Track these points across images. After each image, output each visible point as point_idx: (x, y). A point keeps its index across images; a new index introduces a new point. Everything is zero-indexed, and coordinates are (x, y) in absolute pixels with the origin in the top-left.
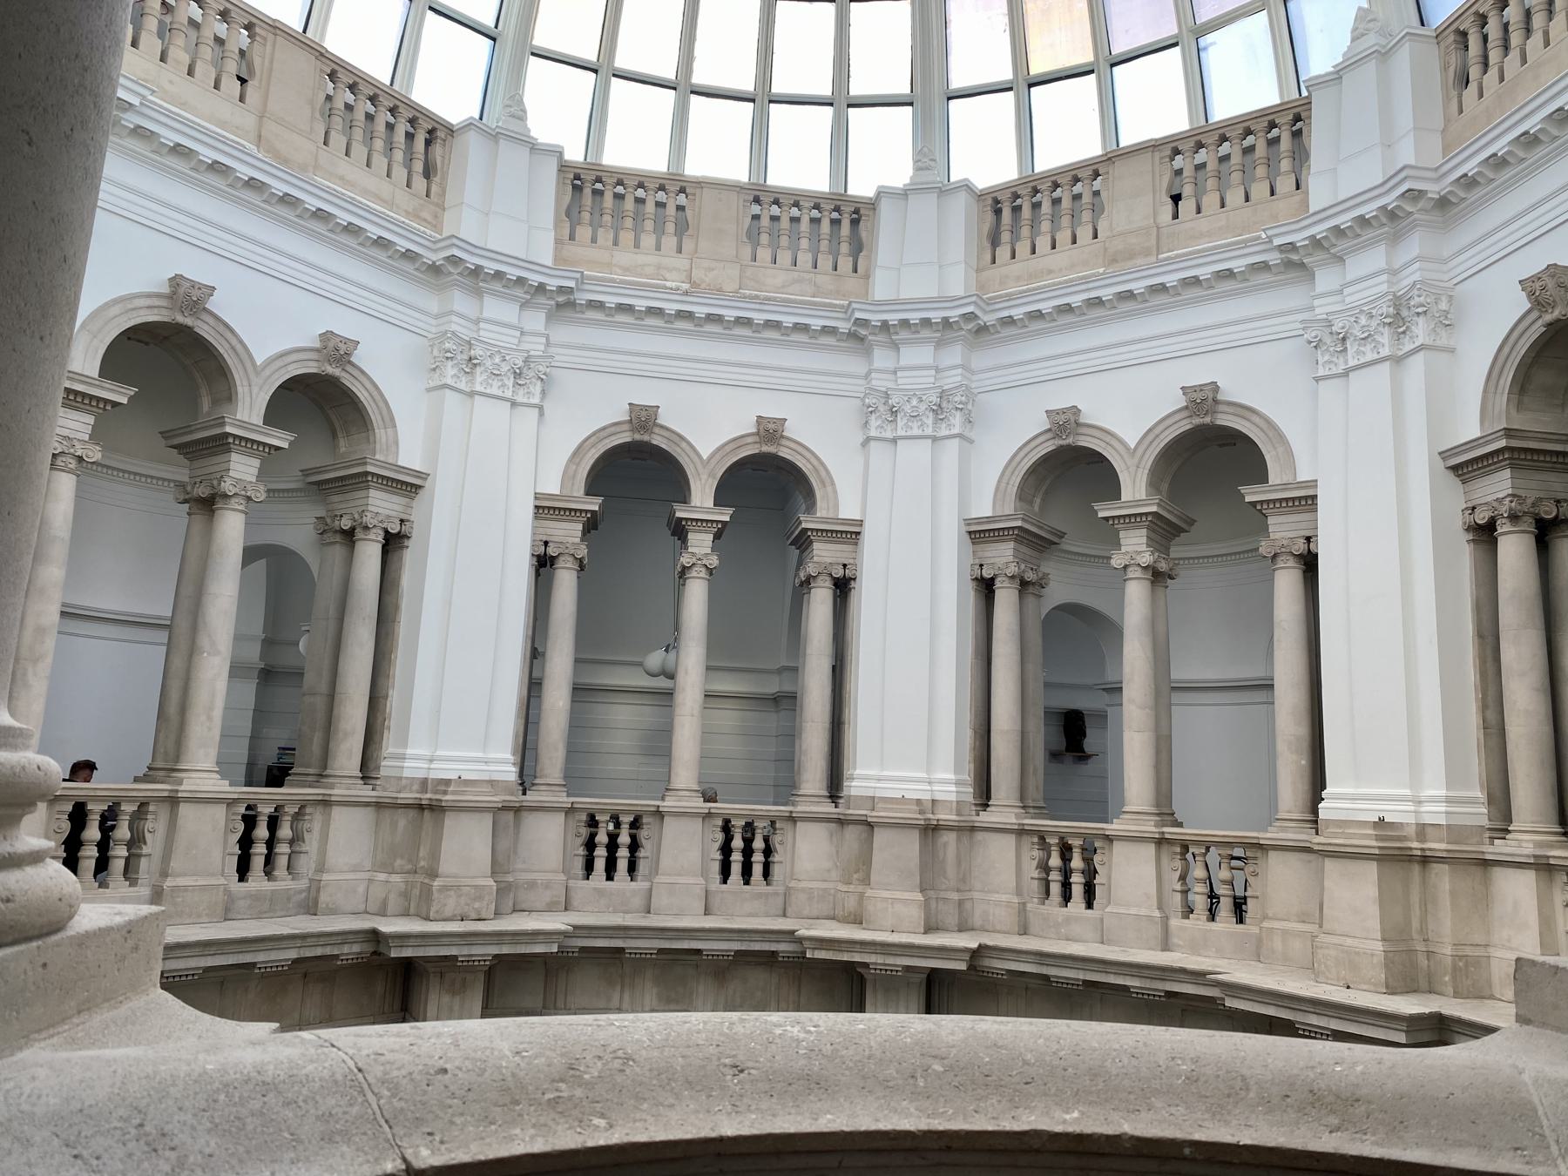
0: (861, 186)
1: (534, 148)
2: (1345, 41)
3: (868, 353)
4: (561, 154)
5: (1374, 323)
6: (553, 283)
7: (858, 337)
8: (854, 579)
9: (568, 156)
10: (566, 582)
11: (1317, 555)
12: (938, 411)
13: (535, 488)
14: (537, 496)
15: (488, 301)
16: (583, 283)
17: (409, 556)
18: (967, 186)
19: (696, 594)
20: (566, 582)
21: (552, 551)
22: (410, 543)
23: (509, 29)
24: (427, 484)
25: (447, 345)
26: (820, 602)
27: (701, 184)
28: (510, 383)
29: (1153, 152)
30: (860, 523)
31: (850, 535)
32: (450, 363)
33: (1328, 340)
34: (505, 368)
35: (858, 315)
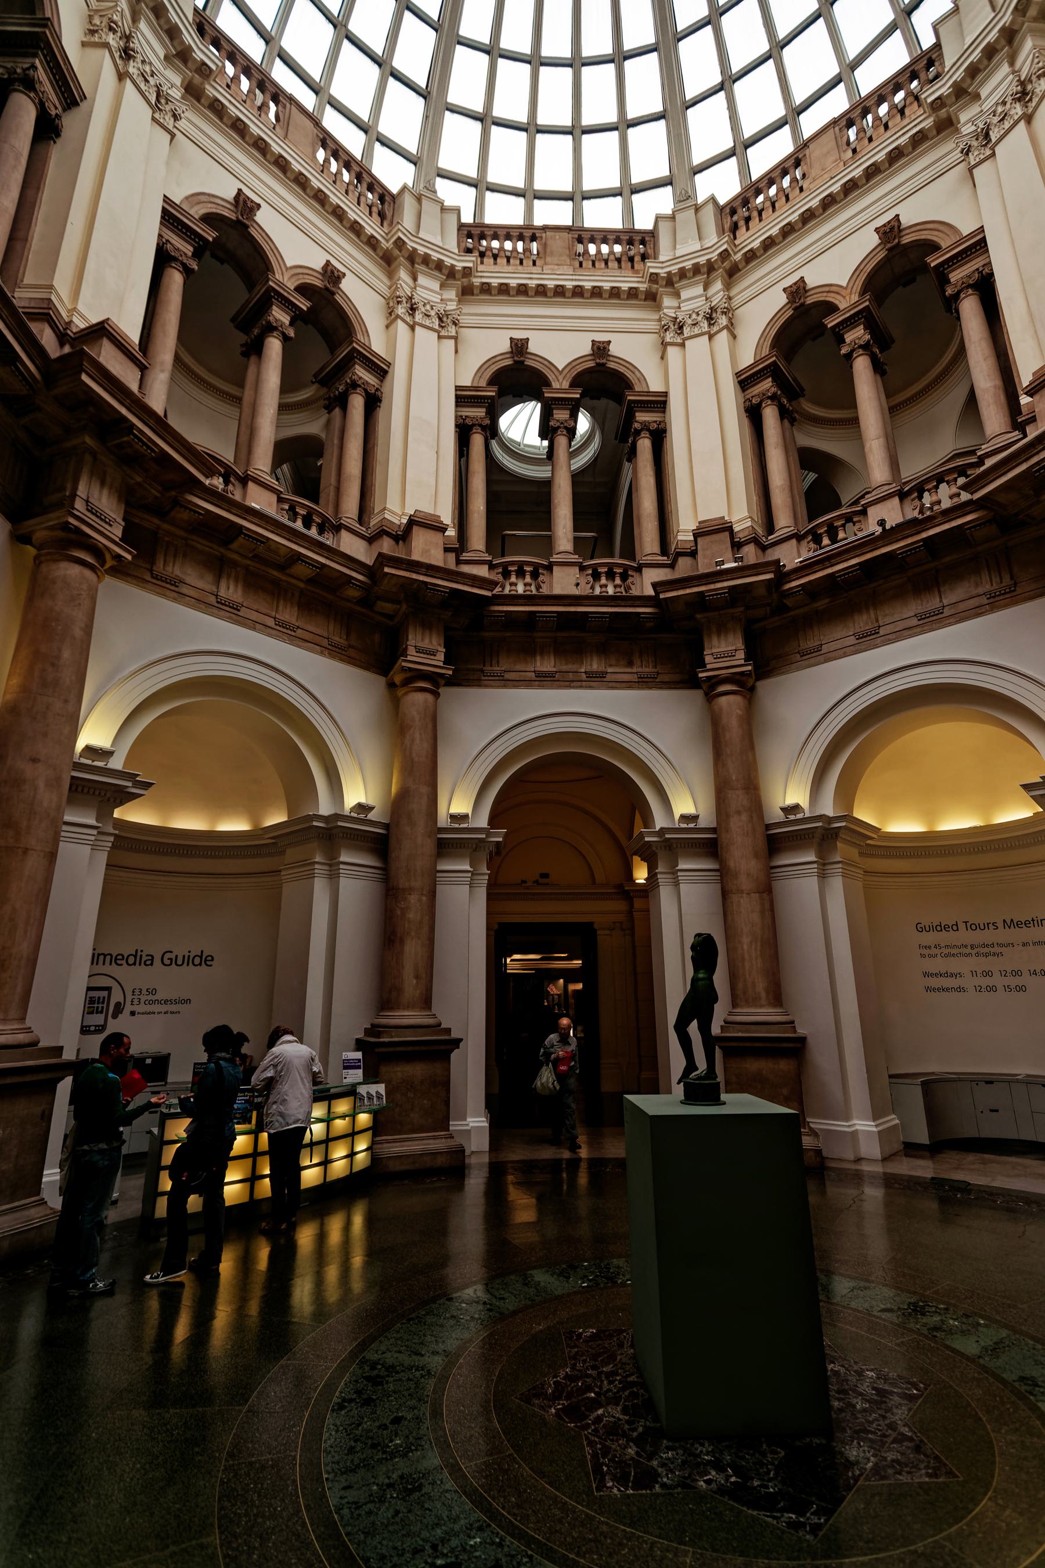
0: (643, 222)
3: (659, 308)
4: (457, 211)
5: (1008, 106)
6: (459, 266)
11: (992, 275)
12: (710, 319)
14: (458, 388)
16: (477, 271)
17: (381, 413)
18: (713, 199)
21: (469, 422)
22: (384, 405)
24: (390, 370)
27: (545, 228)
30: (666, 394)
31: (660, 403)
33: (975, 143)
34: (433, 313)
35: (652, 270)
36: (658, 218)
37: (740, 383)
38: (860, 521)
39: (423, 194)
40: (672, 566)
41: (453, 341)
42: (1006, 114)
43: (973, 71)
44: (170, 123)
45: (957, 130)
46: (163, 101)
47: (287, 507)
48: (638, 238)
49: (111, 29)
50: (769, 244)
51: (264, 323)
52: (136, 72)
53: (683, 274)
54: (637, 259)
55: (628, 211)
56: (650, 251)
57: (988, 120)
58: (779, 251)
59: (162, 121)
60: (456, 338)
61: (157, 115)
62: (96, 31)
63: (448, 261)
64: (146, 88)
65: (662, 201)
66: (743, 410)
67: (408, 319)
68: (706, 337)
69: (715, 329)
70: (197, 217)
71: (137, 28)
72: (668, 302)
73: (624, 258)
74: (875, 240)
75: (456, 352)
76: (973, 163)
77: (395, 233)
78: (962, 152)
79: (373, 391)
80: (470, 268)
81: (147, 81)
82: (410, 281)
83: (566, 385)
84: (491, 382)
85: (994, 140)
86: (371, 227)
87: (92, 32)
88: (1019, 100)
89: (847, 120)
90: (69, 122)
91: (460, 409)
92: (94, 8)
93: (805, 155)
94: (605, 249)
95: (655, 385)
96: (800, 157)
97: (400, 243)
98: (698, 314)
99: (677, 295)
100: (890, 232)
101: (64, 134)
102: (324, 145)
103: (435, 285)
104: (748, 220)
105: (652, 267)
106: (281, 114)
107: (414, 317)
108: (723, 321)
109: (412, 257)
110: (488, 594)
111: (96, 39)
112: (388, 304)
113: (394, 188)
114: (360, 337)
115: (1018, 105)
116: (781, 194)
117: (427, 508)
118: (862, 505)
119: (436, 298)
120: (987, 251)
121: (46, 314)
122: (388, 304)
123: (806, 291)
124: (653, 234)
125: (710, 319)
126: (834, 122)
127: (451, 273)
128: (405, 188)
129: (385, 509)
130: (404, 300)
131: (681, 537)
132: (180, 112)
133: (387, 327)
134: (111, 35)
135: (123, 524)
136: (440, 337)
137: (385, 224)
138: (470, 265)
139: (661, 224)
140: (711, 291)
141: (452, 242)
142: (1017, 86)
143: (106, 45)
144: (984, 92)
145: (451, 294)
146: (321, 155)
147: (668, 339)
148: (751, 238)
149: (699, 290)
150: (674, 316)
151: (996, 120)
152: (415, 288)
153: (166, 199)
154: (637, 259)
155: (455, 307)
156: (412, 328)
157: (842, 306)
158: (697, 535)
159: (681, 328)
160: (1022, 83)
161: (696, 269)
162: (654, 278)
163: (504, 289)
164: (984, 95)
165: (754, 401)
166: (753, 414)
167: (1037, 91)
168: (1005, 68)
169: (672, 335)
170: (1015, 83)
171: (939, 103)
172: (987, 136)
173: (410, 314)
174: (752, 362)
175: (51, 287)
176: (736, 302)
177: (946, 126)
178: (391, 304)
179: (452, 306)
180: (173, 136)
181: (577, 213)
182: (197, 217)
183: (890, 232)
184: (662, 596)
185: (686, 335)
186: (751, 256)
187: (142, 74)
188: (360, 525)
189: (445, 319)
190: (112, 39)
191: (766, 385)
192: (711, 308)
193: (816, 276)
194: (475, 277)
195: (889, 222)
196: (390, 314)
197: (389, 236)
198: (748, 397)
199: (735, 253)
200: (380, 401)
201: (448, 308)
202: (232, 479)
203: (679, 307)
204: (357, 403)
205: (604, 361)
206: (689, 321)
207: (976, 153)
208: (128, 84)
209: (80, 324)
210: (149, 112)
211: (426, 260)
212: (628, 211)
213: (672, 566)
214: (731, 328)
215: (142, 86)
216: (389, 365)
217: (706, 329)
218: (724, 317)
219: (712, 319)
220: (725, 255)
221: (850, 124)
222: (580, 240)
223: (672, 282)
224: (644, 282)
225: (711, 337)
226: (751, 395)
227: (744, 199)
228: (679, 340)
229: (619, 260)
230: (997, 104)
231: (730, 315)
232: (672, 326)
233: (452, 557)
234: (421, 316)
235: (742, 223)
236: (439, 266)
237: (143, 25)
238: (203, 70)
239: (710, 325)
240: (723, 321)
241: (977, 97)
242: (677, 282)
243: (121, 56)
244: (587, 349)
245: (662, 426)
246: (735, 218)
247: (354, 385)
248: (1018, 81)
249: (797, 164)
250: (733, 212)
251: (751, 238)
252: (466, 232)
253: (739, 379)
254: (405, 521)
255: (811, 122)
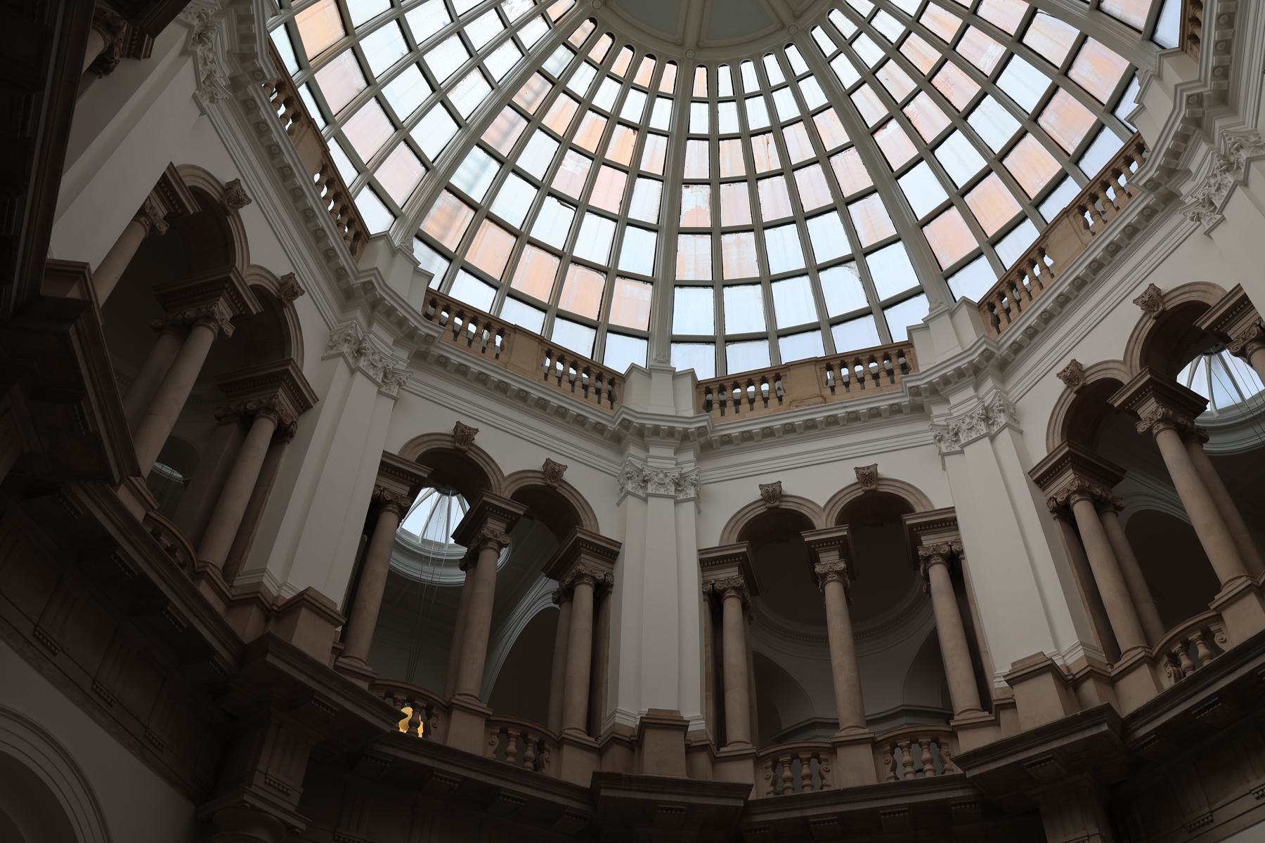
0: (900, 336)
1: (676, 376)
2: (1139, 87)
4: (692, 373)
5: (1219, 178)
7: (918, 410)
8: (962, 552)
9: (701, 377)
10: (732, 609)
12: (987, 418)
13: (697, 546)
15: (654, 451)
18: (965, 301)
19: (834, 594)
20: (732, 609)
22: (614, 590)
23: (655, 331)
24: (621, 550)
25: (627, 469)
26: (938, 575)
28: (673, 488)
29: (1068, 216)
31: (947, 522)
32: (630, 481)
33: (1203, 211)
36: (910, 330)
37: (1037, 481)
38: (1220, 630)
39: (659, 366)
40: (996, 723)
41: (692, 504)
42: (1220, 184)
43: (1174, 154)
44: (395, 391)
45: (1183, 203)
46: (390, 376)
47: (497, 731)
48: (893, 352)
49: (346, 341)
50: (1032, 333)
51: (479, 537)
52: (366, 363)
53: (946, 381)
54: (897, 371)
55: (883, 328)
56: (909, 363)
57: (1206, 192)
58: (1043, 341)
59: (387, 392)
60: (697, 500)
61: (383, 389)
62: (335, 346)
63: (679, 426)
64: (374, 372)
65: (918, 310)
66: (1047, 510)
67: (641, 493)
68: (987, 440)
69: (996, 428)
70: (414, 461)
71: (370, 332)
72: (937, 410)
73: (883, 374)
74: (1138, 312)
75: (699, 512)
76: (1207, 227)
77: (621, 414)
78: (1192, 219)
79: (603, 577)
80: (704, 427)
81: (375, 366)
82: (642, 454)
83: (831, 524)
84: (741, 538)
85: (1218, 206)
86: (596, 412)
87: (331, 348)
88: (1227, 170)
89: (1078, 207)
90: (303, 424)
91: (708, 573)
92: (336, 328)
93: (1047, 245)
94: (859, 368)
95: (940, 502)
96: (1043, 247)
97: (626, 424)
98: (972, 418)
99: (947, 401)
100: (1152, 300)
101: (296, 436)
102: (549, 355)
103: (669, 452)
104: (1008, 311)
105: (911, 381)
106: (505, 344)
107: (647, 489)
108: (1002, 419)
109: (641, 432)
110: (741, 804)
111: (333, 352)
112: (619, 481)
113: (622, 369)
114: (587, 524)
115: (1228, 175)
116: (1034, 282)
117: (664, 702)
118: (1215, 609)
119: (670, 465)
120: (1253, 308)
121: (255, 598)
122: (619, 481)
123: (1084, 372)
124: (909, 344)
125: (987, 418)
126: (1066, 212)
127: (685, 437)
128: (633, 368)
129: (616, 711)
130: (635, 474)
131: (996, 685)
132: (404, 379)
133: (618, 504)
134: (346, 345)
135: (301, 790)
136: (677, 503)
137: (615, 404)
138: (704, 424)
139: (914, 335)
140: (983, 391)
141: (687, 406)
142: (1219, 160)
143: (342, 354)
144: (1193, 167)
145: (689, 456)
146: (548, 362)
147: (944, 450)
148: (1014, 332)
149: (970, 392)
150: (945, 423)
151: (1213, 190)
152: (646, 461)
153: (385, 454)
154: (897, 371)
155: (693, 468)
156: (645, 500)
157: (1125, 380)
158: (1013, 680)
159: (956, 434)
160: (1225, 157)
161: (960, 373)
162: (915, 392)
163: (747, 437)
164: (1193, 168)
165: (1059, 500)
166: (1063, 512)
167: (1241, 160)
168: (1204, 147)
169: (947, 444)
170: (1215, 159)
171: (1152, 185)
172: (1212, 203)
173: (642, 487)
174: (1046, 455)
175: (264, 570)
176: (1013, 395)
177: (1170, 199)
178: (622, 481)
179: (688, 468)
180: (396, 400)
181: (829, 342)
182: (414, 461)
183: (1152, 300)
184: (969, 774)
185: (963, 442)
186: (1017, 348)
187: (372, 363)
188: (589, 735)
189: (682, 482)
190: (346, 349)
191: (1068, 479)
192: (986, 409)
193: (1088, 356)
194: (712, 432)
195: (1145, 293)
196: (621, 490)
197: (615, 418)
198: (1051, 495)
199: (999, 349)
200: (612, 586)
201: (684, 471)
202: (434, 711)
203: (951, 414)
204: (585, 594)
205: (874, 487)
206: (964, 427)
207: (1208, 218)
208: (358, 375)
209: (288, 595)
210: (376, 389)
211: (656, 431)
212: (883, 328)
213: (996, 723)
214: (1014, 424)
215: (371, 373)
216: (619, 545)
217: (985, 432)
218: (1002, 414)
219: (990, 419)
220: (988, 356)
221: (1083, 210)
222: (829, 368)
223: (939, 390)
224: (906, 396)
225: (992, 439)
226: (1055, 492)
227: (996, 293)
228: (957, 448)
229: (876, 377)
230: (1207, 177)
231: (1012, 410)
232: (947, 436)
233: (702, 760)
234: (654, 486)
235: (1002, 317)
236: (671, 432)
237: (376, 328)
238: (429, 339)
239: (988, 426)
240: (1002, 419)
241: (1189, 171)
242: (942, 390)
243: (354, 356)
244: (852, 478)
245: (955, 547)
246: (996, 312)
247: (580, 576)
248: (1217, 156)
249: (1042, 253)
250: (992, 307)
251: (1014, 332)
252: (704, 389)
253: (1034, 478)
254: (638, 723)
255: (1050, 210)
